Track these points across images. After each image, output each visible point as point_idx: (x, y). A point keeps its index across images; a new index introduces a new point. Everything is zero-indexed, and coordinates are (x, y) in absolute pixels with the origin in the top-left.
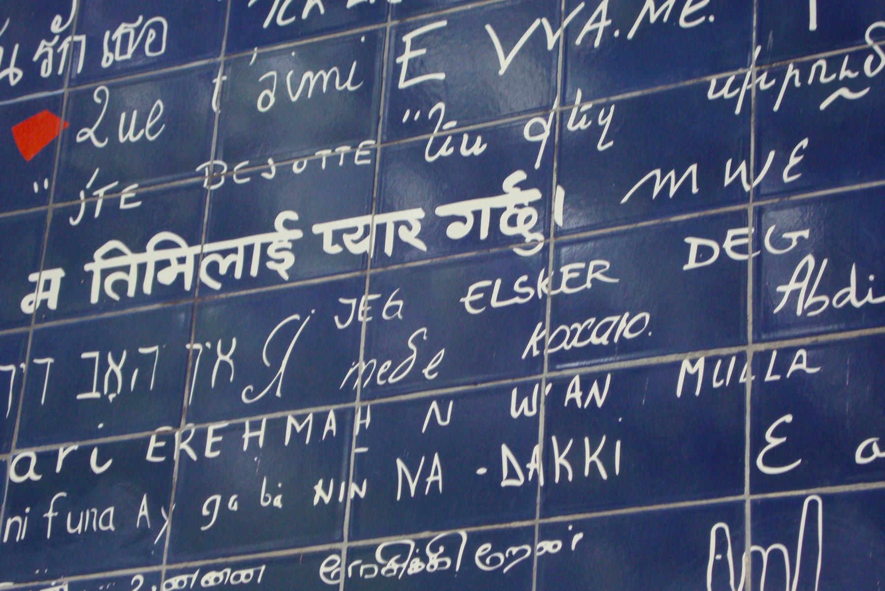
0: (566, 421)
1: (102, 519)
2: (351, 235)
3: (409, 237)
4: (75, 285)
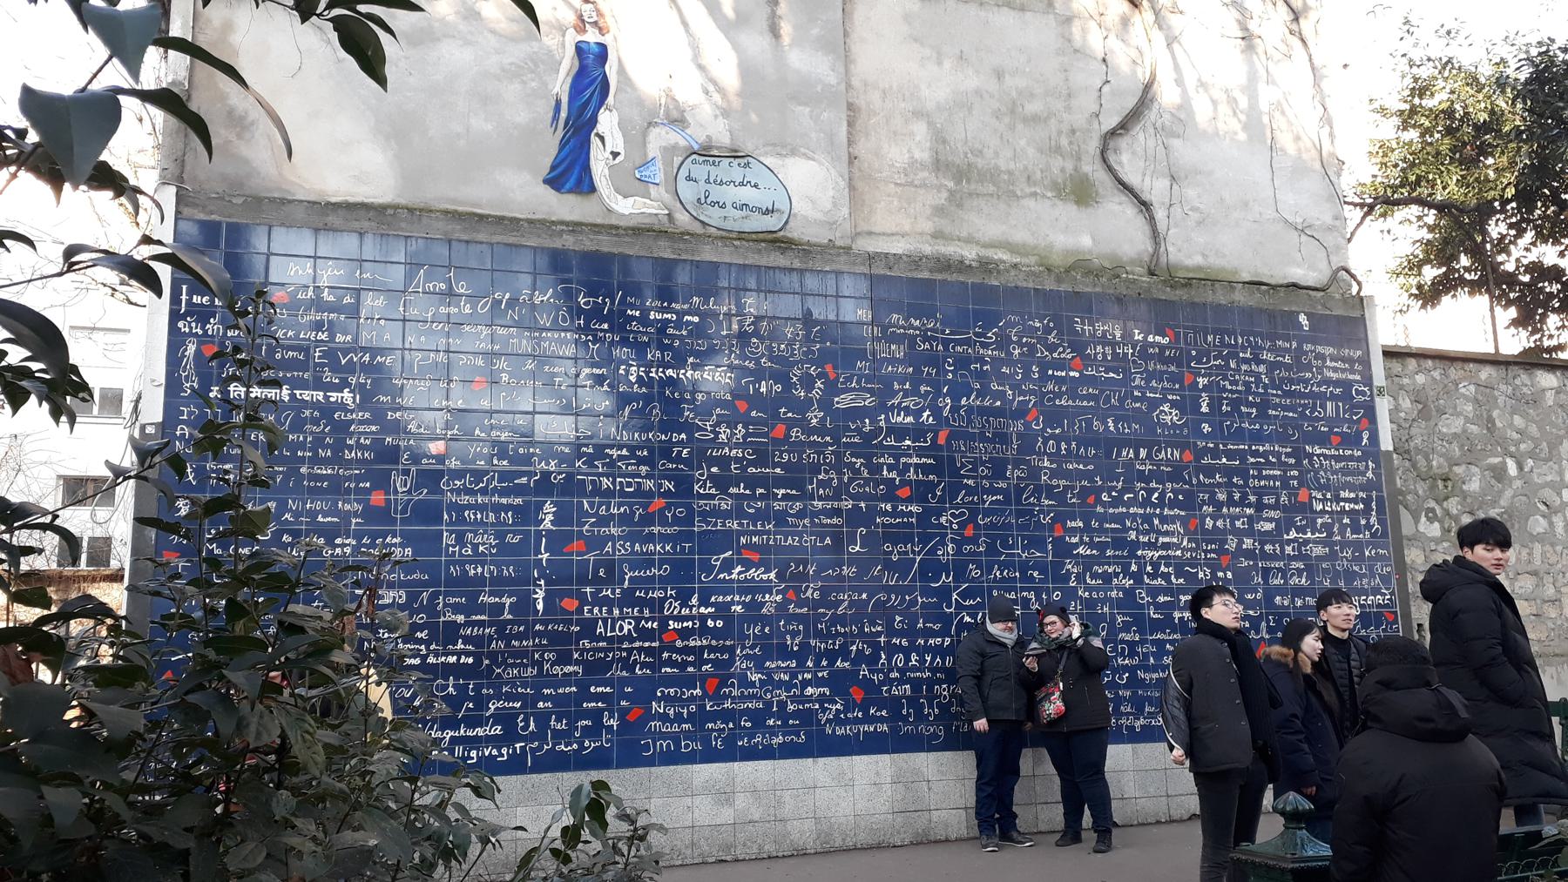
0: (359, 446)
2: (307, 395)
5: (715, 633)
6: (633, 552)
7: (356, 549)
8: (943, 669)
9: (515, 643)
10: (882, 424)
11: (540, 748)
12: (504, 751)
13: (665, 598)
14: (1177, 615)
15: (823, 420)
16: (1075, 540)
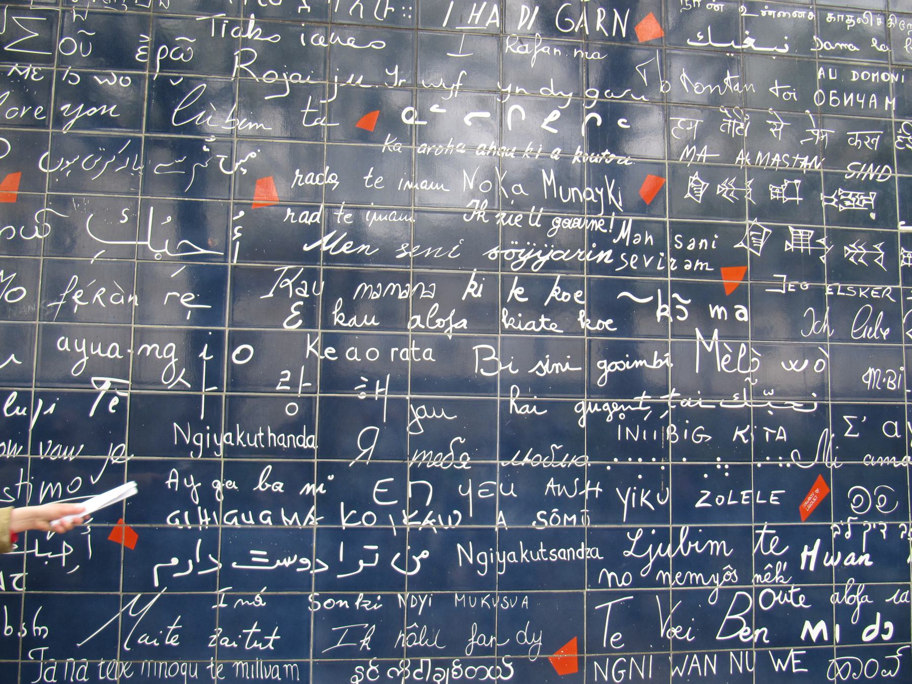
14: (585, 408)
16: (307, 218)
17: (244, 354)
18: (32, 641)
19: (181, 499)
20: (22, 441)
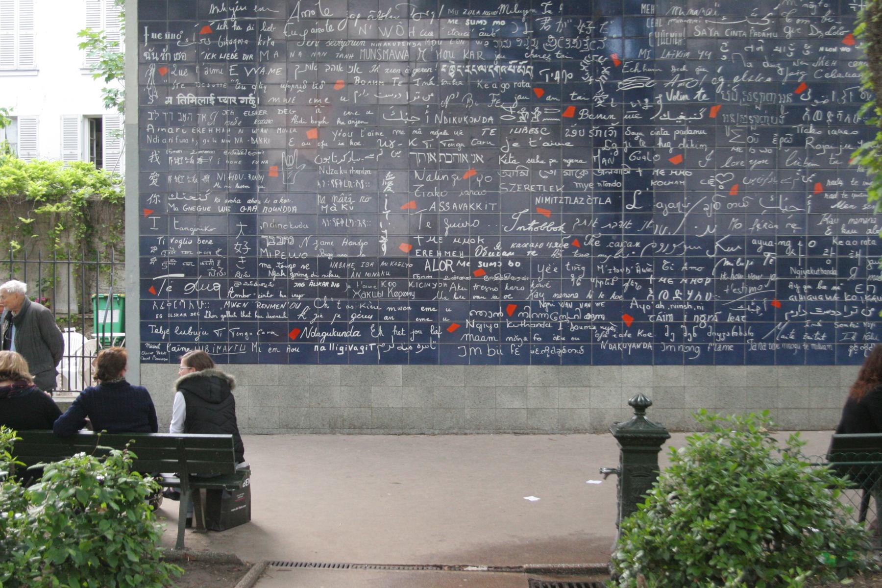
1: (186, 141)
2: (225, 99)
3: (234, 101)
4: (175, 100)
5: (515, 271)
6: (451, 210)
7: (261, 207)
8: (704, 303)
9: (368, 274)
10: (660, 102)
11: (386, 348)
12: (362, 348)
13: (476, 245)
15: (608, 100)
16: (833, 197)
17: (813, 244)
18: (749, 337)
19: (793, 292)
20: (742, 273)
